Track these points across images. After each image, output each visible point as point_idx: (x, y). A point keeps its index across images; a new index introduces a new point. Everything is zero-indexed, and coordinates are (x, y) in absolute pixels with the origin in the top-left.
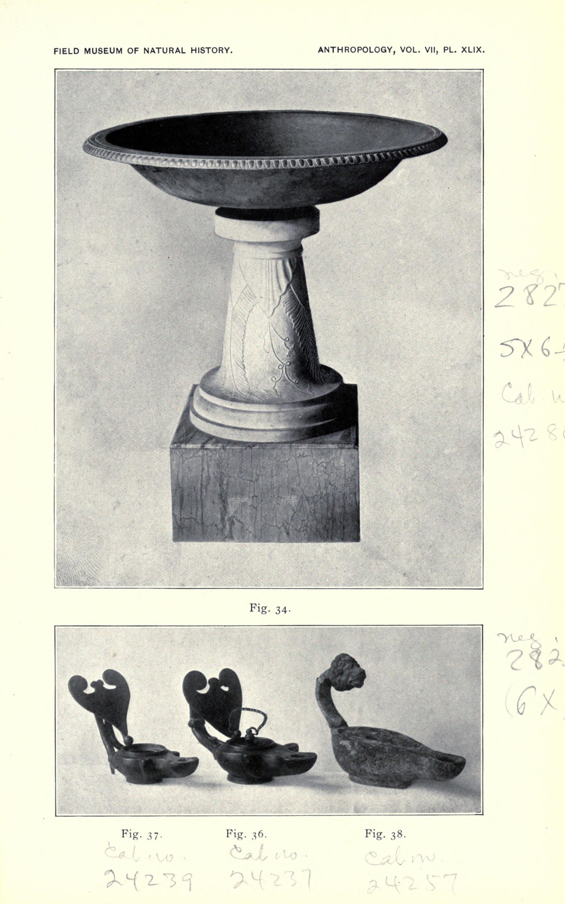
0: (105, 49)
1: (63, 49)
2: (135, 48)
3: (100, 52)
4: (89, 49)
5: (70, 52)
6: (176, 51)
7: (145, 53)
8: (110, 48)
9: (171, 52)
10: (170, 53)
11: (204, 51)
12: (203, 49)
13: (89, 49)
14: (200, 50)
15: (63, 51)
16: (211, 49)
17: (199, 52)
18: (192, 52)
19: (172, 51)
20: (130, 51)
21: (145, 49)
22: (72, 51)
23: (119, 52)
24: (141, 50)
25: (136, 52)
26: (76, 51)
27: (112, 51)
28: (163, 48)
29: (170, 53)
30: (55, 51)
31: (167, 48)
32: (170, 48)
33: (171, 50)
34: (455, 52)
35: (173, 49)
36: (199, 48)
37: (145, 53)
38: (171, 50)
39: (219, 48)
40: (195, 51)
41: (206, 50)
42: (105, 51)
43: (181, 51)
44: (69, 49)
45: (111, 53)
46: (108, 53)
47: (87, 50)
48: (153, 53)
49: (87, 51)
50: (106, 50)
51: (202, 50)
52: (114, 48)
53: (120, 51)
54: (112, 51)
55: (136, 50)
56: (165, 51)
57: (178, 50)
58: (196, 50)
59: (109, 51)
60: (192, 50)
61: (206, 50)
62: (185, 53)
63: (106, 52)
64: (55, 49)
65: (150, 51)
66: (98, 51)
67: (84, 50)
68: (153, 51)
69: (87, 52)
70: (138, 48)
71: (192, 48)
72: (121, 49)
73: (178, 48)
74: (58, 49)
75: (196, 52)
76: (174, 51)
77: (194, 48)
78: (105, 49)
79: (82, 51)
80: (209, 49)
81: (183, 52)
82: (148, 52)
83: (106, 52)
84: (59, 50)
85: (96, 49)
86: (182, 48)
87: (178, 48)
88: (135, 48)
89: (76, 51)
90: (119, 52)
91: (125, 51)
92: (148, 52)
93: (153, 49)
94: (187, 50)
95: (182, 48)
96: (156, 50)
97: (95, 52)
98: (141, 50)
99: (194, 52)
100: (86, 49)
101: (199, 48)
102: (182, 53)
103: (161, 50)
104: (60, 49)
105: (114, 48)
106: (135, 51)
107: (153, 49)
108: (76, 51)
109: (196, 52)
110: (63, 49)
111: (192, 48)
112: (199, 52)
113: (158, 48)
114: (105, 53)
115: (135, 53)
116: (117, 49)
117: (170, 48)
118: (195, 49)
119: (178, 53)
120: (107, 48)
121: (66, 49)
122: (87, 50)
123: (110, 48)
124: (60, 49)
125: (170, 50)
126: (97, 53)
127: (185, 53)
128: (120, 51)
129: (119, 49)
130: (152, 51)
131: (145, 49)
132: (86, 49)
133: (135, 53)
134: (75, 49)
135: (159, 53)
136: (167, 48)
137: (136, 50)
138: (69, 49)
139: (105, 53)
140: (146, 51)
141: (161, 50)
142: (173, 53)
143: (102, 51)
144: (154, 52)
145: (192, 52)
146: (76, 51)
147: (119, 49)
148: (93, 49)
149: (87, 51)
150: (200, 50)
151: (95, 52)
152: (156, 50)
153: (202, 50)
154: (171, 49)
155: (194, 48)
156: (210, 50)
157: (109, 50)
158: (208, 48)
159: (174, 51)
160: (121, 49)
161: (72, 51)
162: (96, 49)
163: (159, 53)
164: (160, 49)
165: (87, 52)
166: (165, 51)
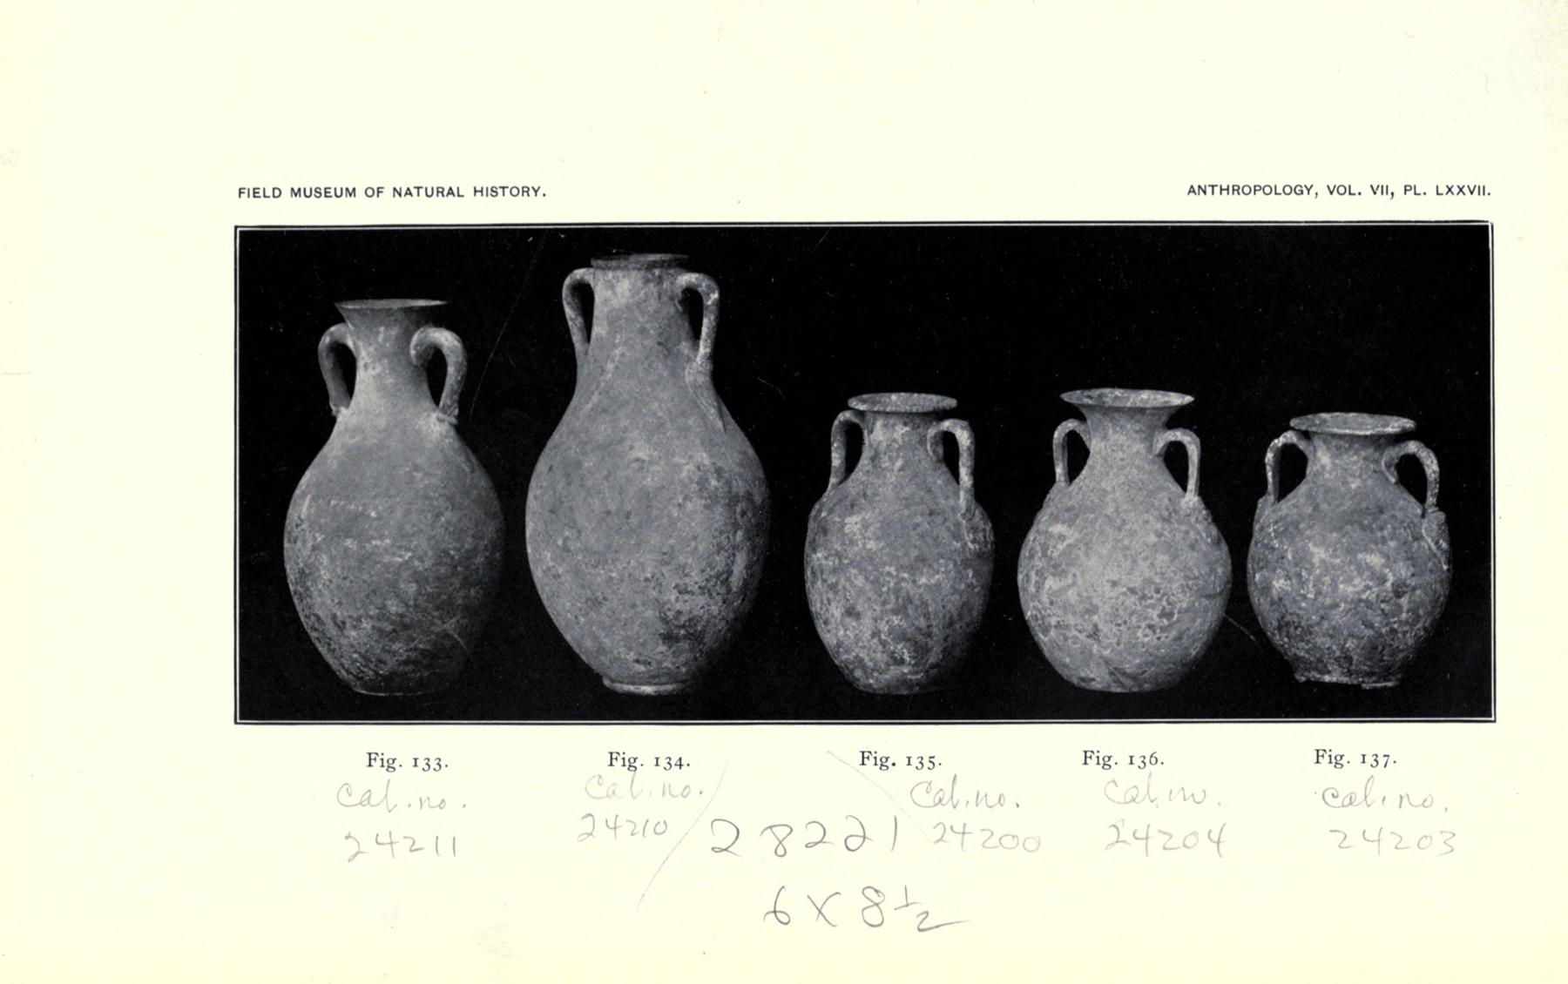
0: (325, 189)
1: (254, 189)
2: (378, 188)
3: (318, 195)
4: (299, 190)
5: (267, 194)
6: (449, 194)
7: (394, 196)
8: (335, 189)
9: (440, 194)
10: (438, 196)
11: (497, 192)
12: (494, 189)
13: (299, 190)
14: (490, 191)
15: (254, 193)
16: (509, 190)
17: (487, 195)
18: (475, 195)
19: (442, 192)
20: (370, 192)
21: (395, 189)
22: (269, 193)
23: (350, 195)
24: (388, 191)
25: (380, 194)
26: (277, 193)
27: (339, 193)
28: (426, 189)
29: (438, 196)
30: (240, 193)
31: (432, 189)
32: (438, 188)
33: (440, 191)
34: (1360, 194)
35: (443, 189)
36: (487, 188)
37: (394, 196)
38: (440, 191)
39: (523, 188)
40: (480, 194)
41: (500, 191)
42: (326, 192)
43: (455, 192)
44: (264, 189)
45: (336, 196)
46: (331, 197)
47: (296, 190)
48: (408, 196)
49: (296, 193)
50: (328, 190)
51: (494, 192)
52: (342, 189)
53: (352, 193)
54: (339, 193)
55: (379, 191)
56: (429, 193)
57: (451, 192)
58: (482, 191)
59: (332, 194)
60: (476, 191)
61: (500, 191)
62: (462, 196)
63: (328, 194)
64: (240, 189)
65: (403, 193)
66: (313, 192)
67: (290, 191)
68: (409, 192)
69: (296, 195)
70: (382, 188)
71: (475, 188)
72: (354, 189)
73: (451, 189)
74: (244, 189)
75: (482, 195)
76: (445, 193)
77: (479, 188)
78: (325, 189)
79: (286, 192)
80: (506, 190)
81: (461, 194)
82: (400, 195)
83: (328, 194)
84: (246, 191)
85: (311, 189)
86: (458, 189)
87: (451, 189)
88: (378, 188)
89: (277, 193)
90: (350, 195)
91: (360, 192)
92: (400, 195)
93: (408, 189)
94: (467, 191)
95: (458, 189)
96: (414, 192)
97: (308, 194)
98: (388, 191)
99: (479, 194)
100: (292, 189)
101: (487, 188)
102: (459, 196)
103: (422, 191)
104: (249, 190)
105: (342, 189)
106: (378, 192)
107: (408, 189)
108: (277, 193)
109: (482, 195)
110: (254, 189)
111: (475, 188)
112: (487, 195)
113: (418, 188)
114: (326, 196)
115: (378, 196)
116: (347, 189)
117: (438, 188)
118: (480, 189)
119: (451, 196)
120: (330, 188)
121: (259, 189)
122: (296, 190)
123: (335, 189)
124: (249, 190)
125: (438, 192)
126: (313, 196)
127: (462, 196)
128: (352, 193)
129: (351, 190)
130: (406, 194)
131: (395, 189)
132: (292, 189)
133: (378, 196)
134: (274, 189)
135: (418, 195)
136: (432, 189)
137: (379, 191)
138: (264, 189)
139: (326, 196)
140: (396, 194)
141: (422, 191)
142: (443, 196)
143: (320, 193)
144: (411, 194)
145: (475, 195)
146: (277, 193)
147: (351, 190)
148: (305, 189)
149: (296, 193)
150: (490, 191)
151: (308, 194)
152: (414, 192)
153: (494, 192)
154: (441, 190)
155: (479, 188)
156: (507, 191)
157: (332, 191)
158: (503, 188)
159: (445, 193)
160: (354, 189)
161: (269, 193)
162: (311, 189)
163: (418, 195)
164: (420, 190)
165: (296, 195)
166: (429, 193)
